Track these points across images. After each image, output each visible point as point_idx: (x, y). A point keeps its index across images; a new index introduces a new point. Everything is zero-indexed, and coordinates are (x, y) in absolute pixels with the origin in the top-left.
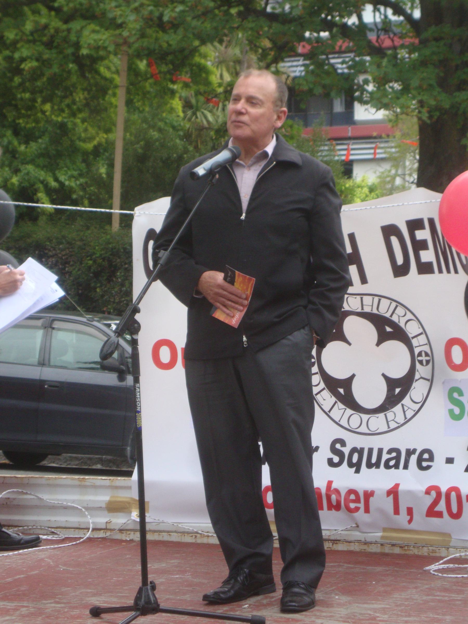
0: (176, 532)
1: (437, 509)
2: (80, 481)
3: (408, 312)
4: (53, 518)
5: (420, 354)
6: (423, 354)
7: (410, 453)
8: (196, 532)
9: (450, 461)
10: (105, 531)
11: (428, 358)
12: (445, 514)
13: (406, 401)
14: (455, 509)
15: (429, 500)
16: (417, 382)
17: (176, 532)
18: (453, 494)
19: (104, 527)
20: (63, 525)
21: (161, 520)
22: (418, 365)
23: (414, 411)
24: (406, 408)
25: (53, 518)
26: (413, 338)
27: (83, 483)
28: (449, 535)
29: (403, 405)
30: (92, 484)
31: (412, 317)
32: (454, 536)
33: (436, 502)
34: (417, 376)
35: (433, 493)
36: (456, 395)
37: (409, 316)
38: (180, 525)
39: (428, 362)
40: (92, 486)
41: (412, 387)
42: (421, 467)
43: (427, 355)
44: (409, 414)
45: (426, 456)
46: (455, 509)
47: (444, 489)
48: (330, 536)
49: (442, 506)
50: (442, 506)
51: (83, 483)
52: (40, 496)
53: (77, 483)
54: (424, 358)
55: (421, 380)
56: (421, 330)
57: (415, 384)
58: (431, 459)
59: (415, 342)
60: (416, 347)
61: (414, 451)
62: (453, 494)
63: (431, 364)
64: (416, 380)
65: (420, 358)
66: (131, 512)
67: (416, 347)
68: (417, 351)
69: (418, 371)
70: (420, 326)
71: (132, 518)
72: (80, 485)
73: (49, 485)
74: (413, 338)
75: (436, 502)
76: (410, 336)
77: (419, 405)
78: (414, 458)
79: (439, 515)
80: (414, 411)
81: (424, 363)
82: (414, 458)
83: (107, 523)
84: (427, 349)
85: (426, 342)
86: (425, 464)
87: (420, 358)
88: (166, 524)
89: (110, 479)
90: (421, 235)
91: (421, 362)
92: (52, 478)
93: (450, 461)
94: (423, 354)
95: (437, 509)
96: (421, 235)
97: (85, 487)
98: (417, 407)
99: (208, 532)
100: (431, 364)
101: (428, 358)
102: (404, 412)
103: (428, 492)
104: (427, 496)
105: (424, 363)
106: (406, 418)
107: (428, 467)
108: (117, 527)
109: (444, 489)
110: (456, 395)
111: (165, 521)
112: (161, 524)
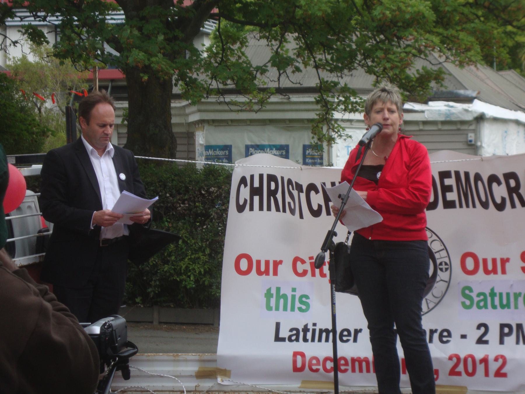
0: (252, 391)
1: (457, 370)
2: (175, 357)
3: (433, 235)
4: (155, 384)
5: (441, 264)
6: (443, 264)
7: (432, 332)
8: (270, 391)
9: (464, 337)
10: (195, 392)
11: (447, 267)
12: (463, 373)
13: (429, 296)
14: (470, 370)
15: (451, 364)
16: (437, 284)
17: (252, 391)
18: (470, 360)
19: (194, 389)
20: (160, 389)
21: (242, 383)
22: (439, 272)
23: (435, 303)
24: (428, 301)
25: (151, 385)
26: (436, 253)
27: (177, 358)
28: (466, 388)
29: (426, 299)
30: (184, 359)
31: (436, 238)
32: (469, 389)
33: (456, 365)
34: (438, 279)
35: (455, 360)
36: (467, 292)
37: (434, 237)
38: (258, 386)
39: (446, 269)
40: (185, 360)
41: (434, 287)
42: (442, 341)
43: (446, 264)
44: (431, 305)
45: (445, 334)
46: (470, 370)
47: (462, 356)
48: (375, 391)
49: (461, 368)
50: (461, 368)
51: (177, 358)
52: (141, 368)
53: (172, 358)
54: (444, 267)
55: (441, 282)
56: (443, 247)
57: (436, 285)
58: (449, 335)
59: (437, 256)
60: (438, 259)
61: (436, 331)
62: (470, 360)
63: (449, 271)
64: (437, 282)
65: (441, 267)
66: (216, 378)
67: (438, 259)
68: (438, 262)
69: (439, 275)
70: (442, 245)
71: (218, 382)
72: (174, 360)
73: (148, 361)
74: (436, 253)
75: (456, 365)
76: (434, 251)
77: (439, 299)
78: (436, 336)
79: (459, 374)
80: (435, 303)
81: (444, 270)
82: (436, 336)
83: (196, 386)
84: (447, 260)
85: (446, 255)
86: (445, 339)
87: (441, 267)
88: (246, 386)
89: (199, 355)
90: (448, 182)
91: (441, 270)
92: (151, 355)
93: (464, 337)
94: (443, 264)
95: (457, 370)
96: (448, 182)
97: (178, 361)
98: (436, 300)
99: (278, 391)
100: (449, 271)
101: (447, 267)
102: (427, 304)
103: (450, 358)
104: (450, 361)
105: (444, 270)
106: (428, 308)
107: (447, 342)
108: (207, 389)
109: (462, 356)
110: (467, 292)
111: (246, 383)
112: (240, 386)
